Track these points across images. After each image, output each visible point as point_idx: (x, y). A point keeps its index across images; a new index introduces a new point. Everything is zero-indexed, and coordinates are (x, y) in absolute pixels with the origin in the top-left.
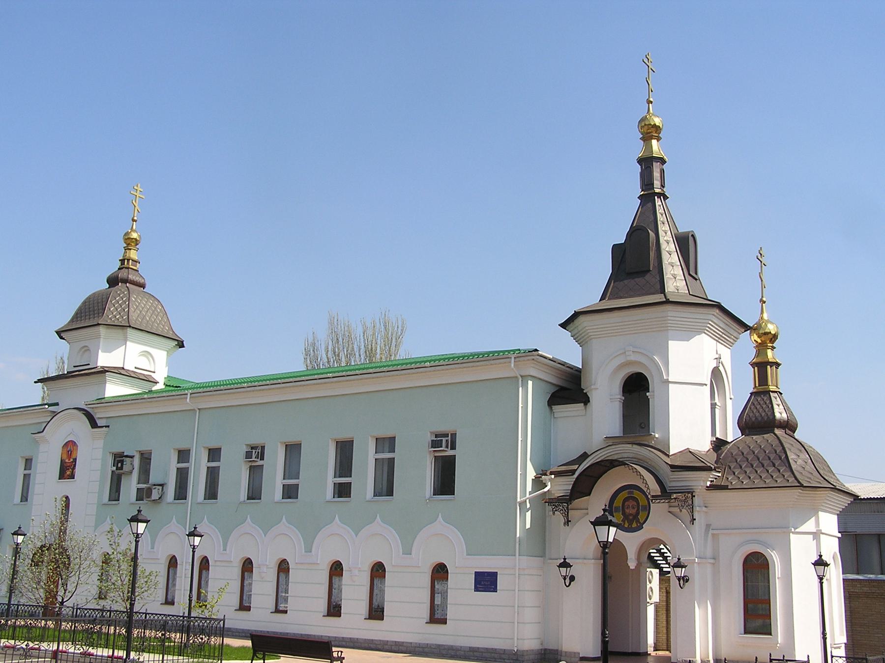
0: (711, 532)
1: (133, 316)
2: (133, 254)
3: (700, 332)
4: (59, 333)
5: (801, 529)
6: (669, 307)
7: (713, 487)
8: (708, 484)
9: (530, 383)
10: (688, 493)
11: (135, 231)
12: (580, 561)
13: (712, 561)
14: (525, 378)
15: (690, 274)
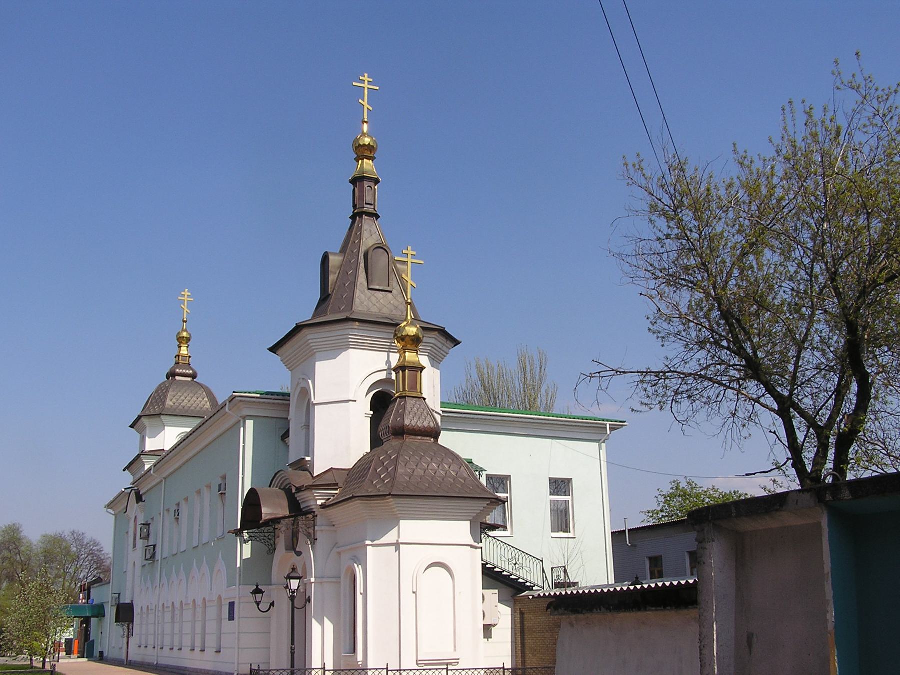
0: (336, 550)
1: (169, 403)
2: (184, 351)
3: (347, 347)
4: (132, 427)
5: (384, 540)
6: (305, 331)
7: (323, 506)
8: (320, 503)
9: (250, 424)
10: (310, 513)
11: (186, 331)
12: (274, 587)
13: (334, 580)
14: (245, 418)
15: (369, 289)
